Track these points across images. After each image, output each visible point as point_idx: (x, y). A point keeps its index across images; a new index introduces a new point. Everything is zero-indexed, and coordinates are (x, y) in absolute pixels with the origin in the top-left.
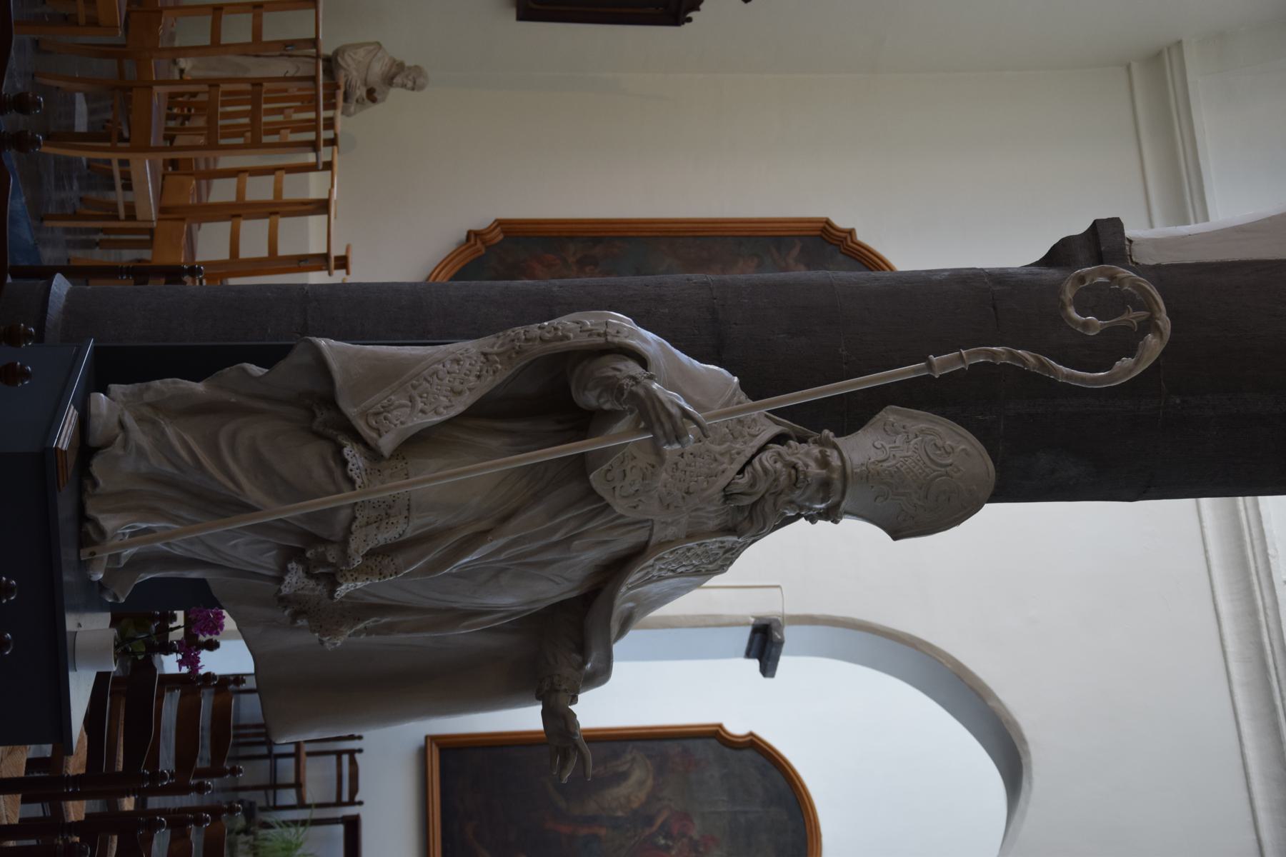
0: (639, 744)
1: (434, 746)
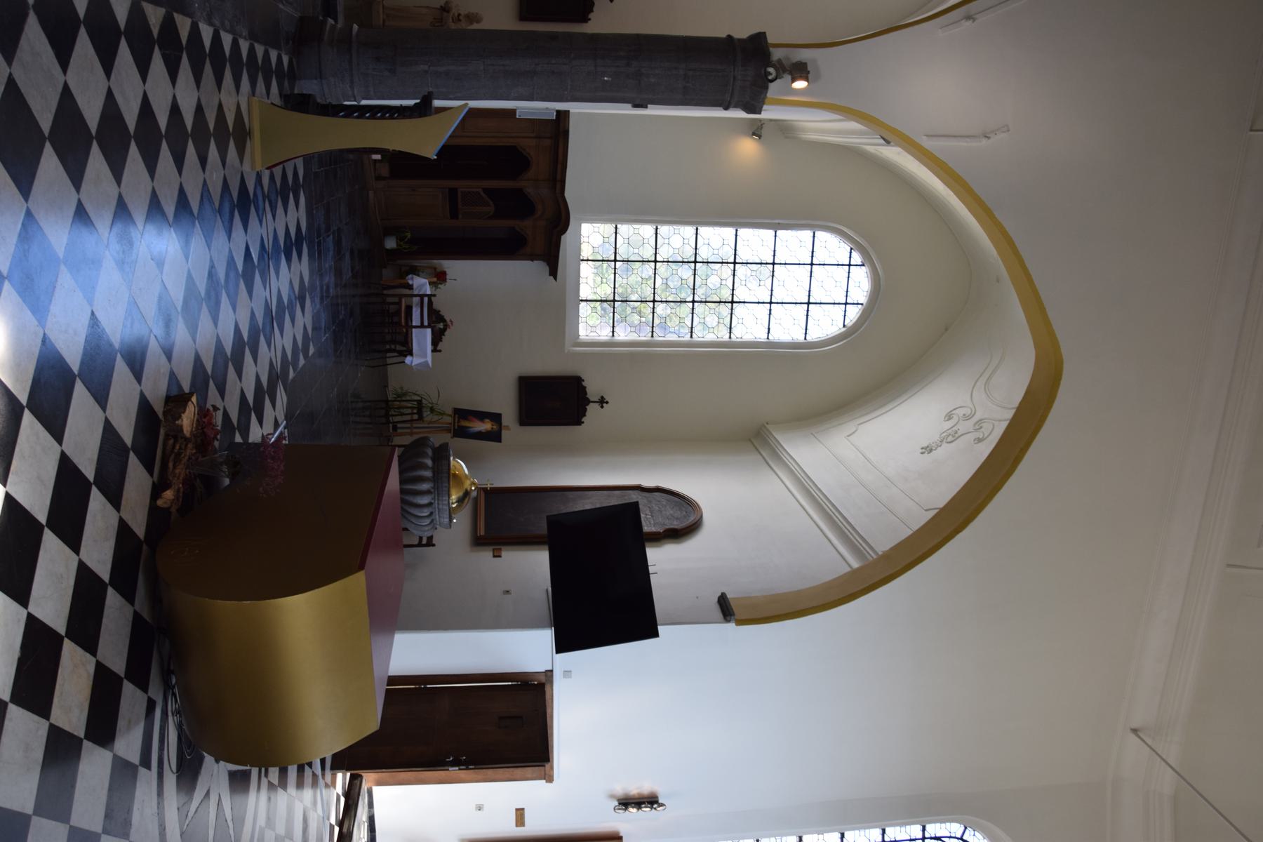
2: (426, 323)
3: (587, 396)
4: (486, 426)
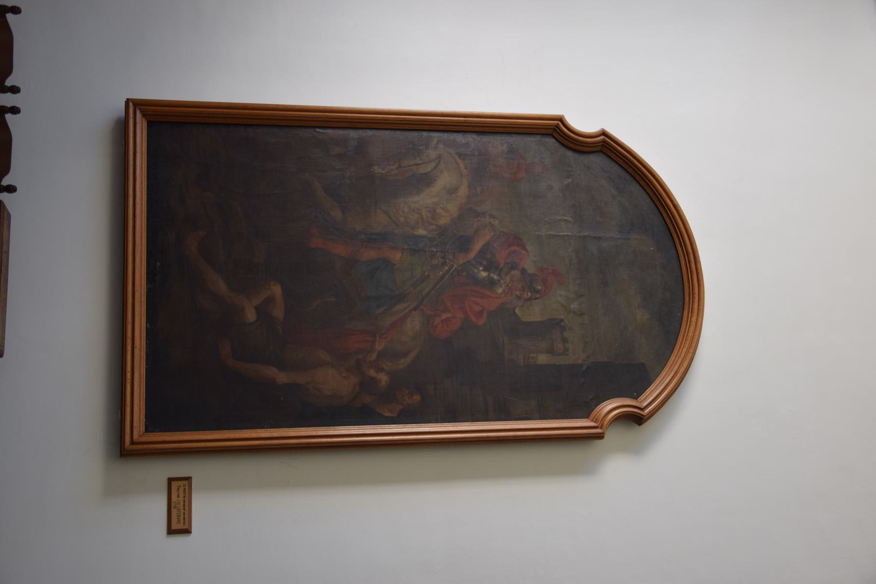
0: (445, 136)
1: (139, 115)
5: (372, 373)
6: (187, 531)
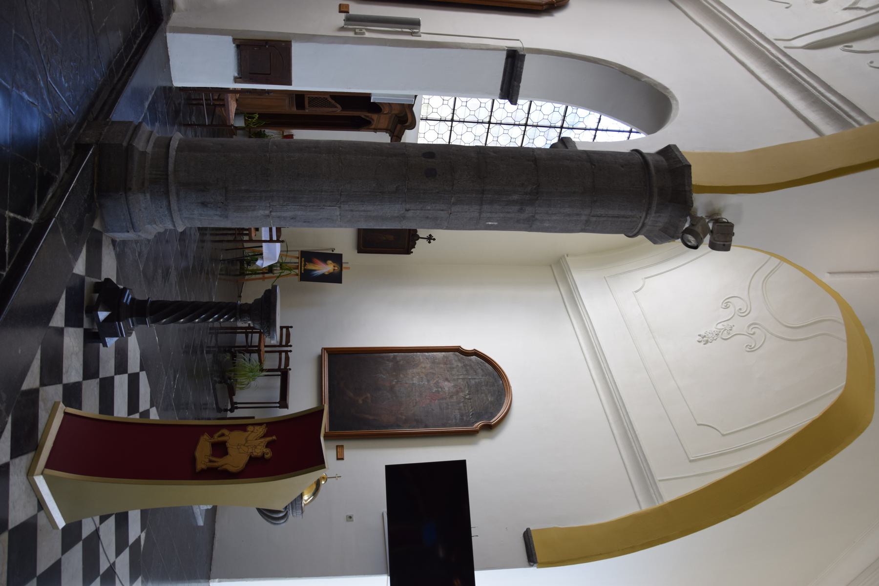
2: (275, 238)
3: (418, 233)
4: (328, 268)
5: (400, 416)
6: (343, 459)
